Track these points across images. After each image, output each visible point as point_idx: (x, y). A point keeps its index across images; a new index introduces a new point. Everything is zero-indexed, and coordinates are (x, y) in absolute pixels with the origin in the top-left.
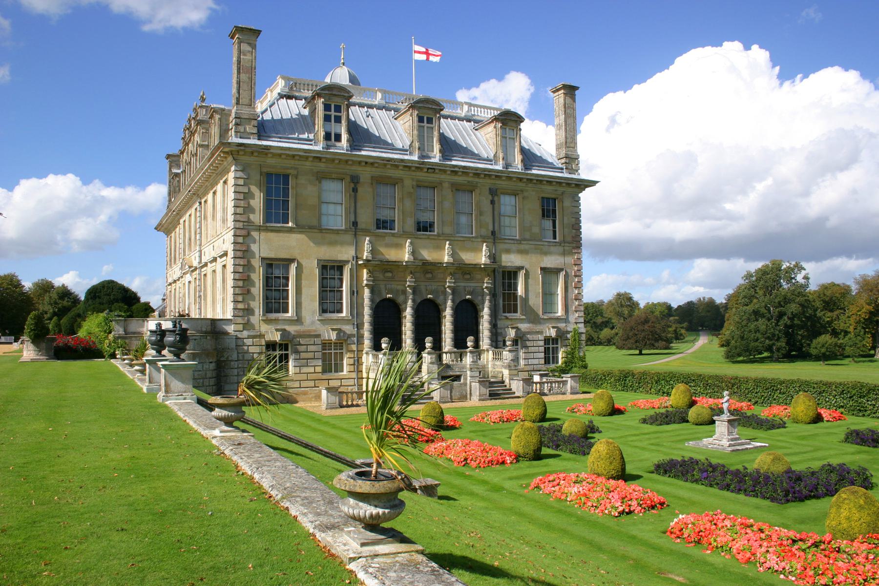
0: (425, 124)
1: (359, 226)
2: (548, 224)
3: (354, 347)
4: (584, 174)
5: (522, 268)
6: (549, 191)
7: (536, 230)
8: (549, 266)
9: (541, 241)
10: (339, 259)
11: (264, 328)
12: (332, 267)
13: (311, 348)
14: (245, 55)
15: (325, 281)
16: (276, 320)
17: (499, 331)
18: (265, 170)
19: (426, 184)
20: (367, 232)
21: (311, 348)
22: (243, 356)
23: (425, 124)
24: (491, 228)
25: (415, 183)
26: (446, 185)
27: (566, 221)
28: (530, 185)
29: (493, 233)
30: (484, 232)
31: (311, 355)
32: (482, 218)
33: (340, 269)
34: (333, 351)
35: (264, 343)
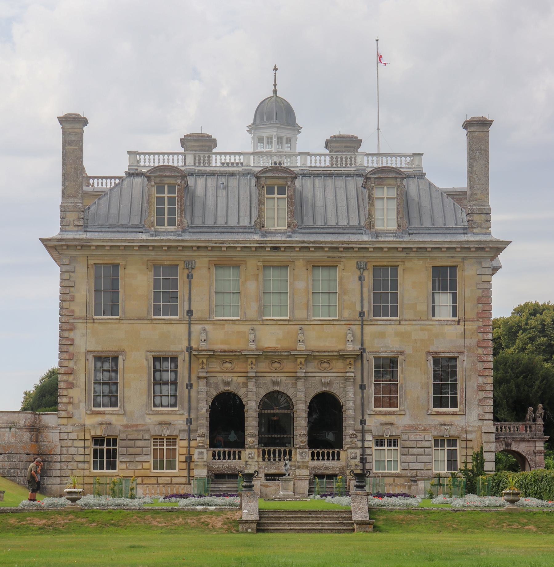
0: (276, 195)
1: (195, 316)
2: (444, 299)
3: (185, 443)
4: (497, 233)
5: (402, 353)
6: (443, 260)
7: (423, 307)
8: (440, 350)
9: (428, 320)
10: (171, 350)
11: (91, 421)
12: (165, 359)
13: (139, 443)
14: (69, 144)
15: (157, 374)
16: (104, 413)
17: (366, 428)
18: (91, 262)
19: (275, 264)
20: (201, 320)
21: (139, 443)
22: (67, 451)
23: (276, 195)
24: (358, 309)
25: (260, 264)
26: (300, 263)
27: (468, 293)
28: (412, 254)
29: (362, 314)
30: (346, 314)
31: (138, 450)
32: (346, 297)
33: (174, 359)
34: (165, 447)
35: (88, 437)
